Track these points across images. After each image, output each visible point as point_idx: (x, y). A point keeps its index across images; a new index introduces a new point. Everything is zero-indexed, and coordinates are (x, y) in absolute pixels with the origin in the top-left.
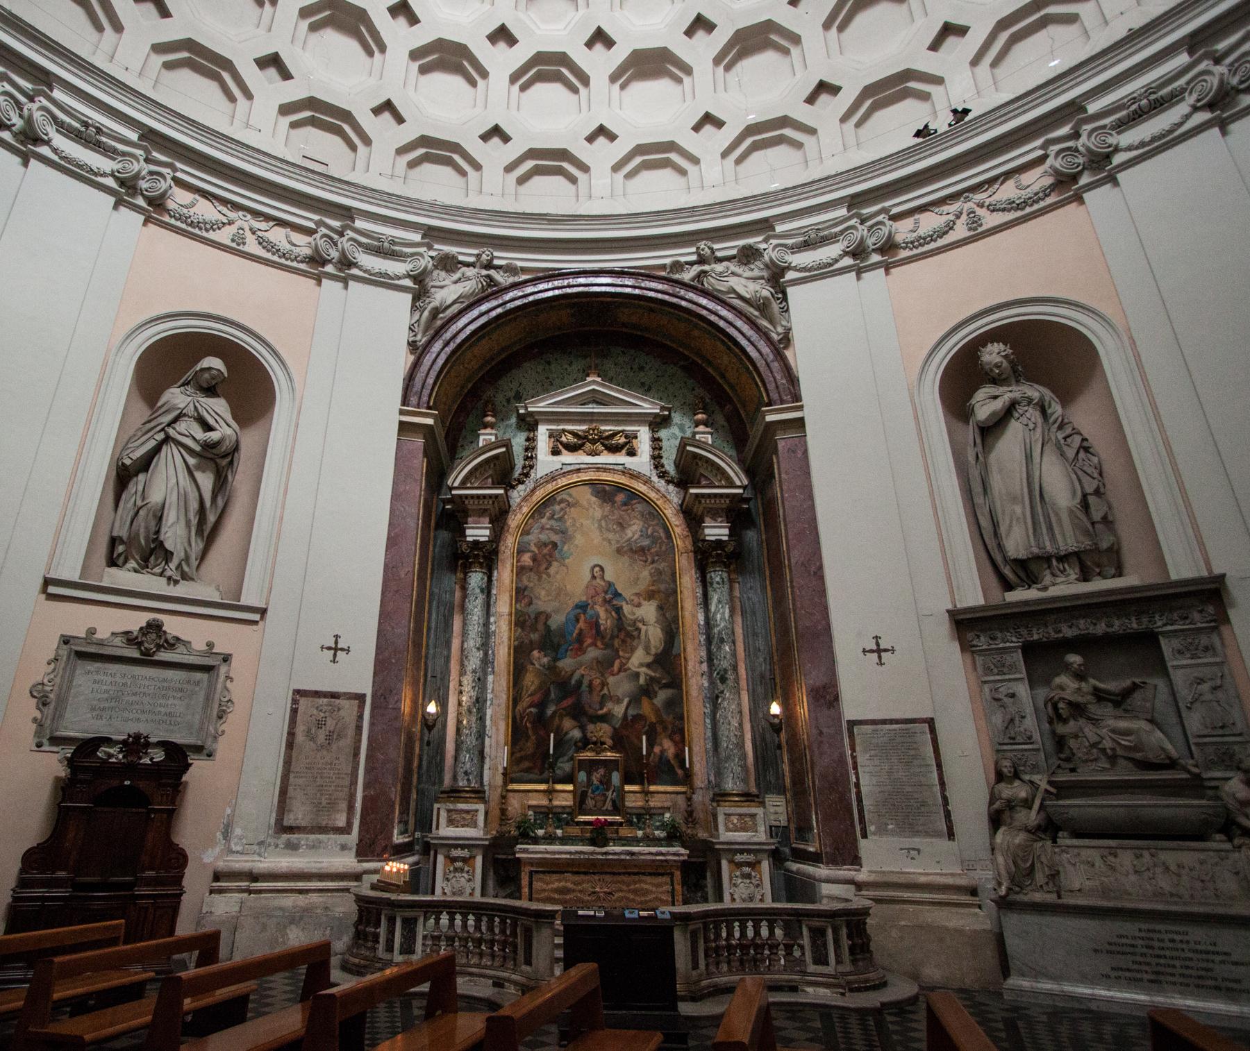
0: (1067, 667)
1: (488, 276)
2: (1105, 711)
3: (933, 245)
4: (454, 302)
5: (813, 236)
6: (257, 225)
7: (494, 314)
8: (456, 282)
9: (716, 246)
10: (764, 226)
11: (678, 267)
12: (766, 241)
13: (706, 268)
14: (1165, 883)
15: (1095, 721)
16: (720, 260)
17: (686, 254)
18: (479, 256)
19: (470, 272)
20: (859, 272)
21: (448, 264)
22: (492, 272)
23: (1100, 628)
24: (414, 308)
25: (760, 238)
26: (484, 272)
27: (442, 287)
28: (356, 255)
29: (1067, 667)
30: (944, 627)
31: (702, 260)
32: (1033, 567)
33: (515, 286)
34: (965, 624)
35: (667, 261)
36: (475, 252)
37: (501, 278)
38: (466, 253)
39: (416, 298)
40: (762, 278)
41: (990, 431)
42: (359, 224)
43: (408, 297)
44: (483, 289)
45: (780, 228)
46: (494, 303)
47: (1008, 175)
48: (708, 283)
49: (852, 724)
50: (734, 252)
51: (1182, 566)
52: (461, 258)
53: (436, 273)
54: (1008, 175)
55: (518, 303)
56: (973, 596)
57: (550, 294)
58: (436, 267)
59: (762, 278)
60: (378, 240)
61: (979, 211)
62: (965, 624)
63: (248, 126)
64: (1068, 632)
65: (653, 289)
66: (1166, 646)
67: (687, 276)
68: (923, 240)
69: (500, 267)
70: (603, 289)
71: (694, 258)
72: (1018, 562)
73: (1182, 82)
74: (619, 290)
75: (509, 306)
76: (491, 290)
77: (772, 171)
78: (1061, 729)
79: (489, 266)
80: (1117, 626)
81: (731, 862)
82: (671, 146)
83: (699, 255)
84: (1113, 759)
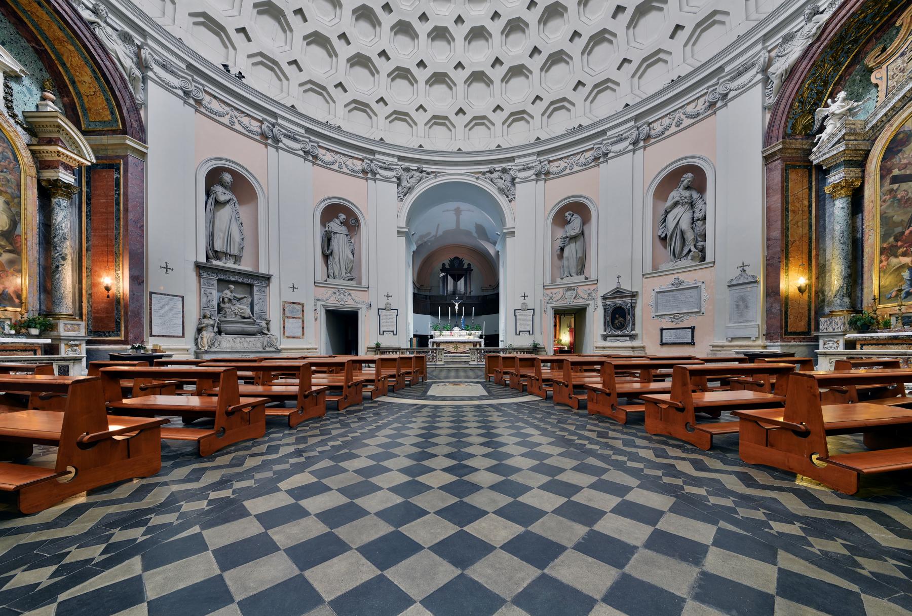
0: (229, 288)
2: (235, 302)
3: (214, 116)
14: (246, 345)
15: (233, 304)
23: (240, 280)
29: (229, 288)
30: (192, 266)
32: (220, 255)
34: (199, 267)
41: (218, 204)
47: (248, 115)
49: (151, 293)
51: (263, 270)
54: (248, 115)
56: (202, 259)
61: (236, 121)
62: (199, 267)
64: (232, 279)
66: (255, 289)
68: (212, 112)
72: (216, 252)
73: (302, 139)
78: (222, 305)
80: (245, 281)
81: (67, 344)
84: (236, 315)
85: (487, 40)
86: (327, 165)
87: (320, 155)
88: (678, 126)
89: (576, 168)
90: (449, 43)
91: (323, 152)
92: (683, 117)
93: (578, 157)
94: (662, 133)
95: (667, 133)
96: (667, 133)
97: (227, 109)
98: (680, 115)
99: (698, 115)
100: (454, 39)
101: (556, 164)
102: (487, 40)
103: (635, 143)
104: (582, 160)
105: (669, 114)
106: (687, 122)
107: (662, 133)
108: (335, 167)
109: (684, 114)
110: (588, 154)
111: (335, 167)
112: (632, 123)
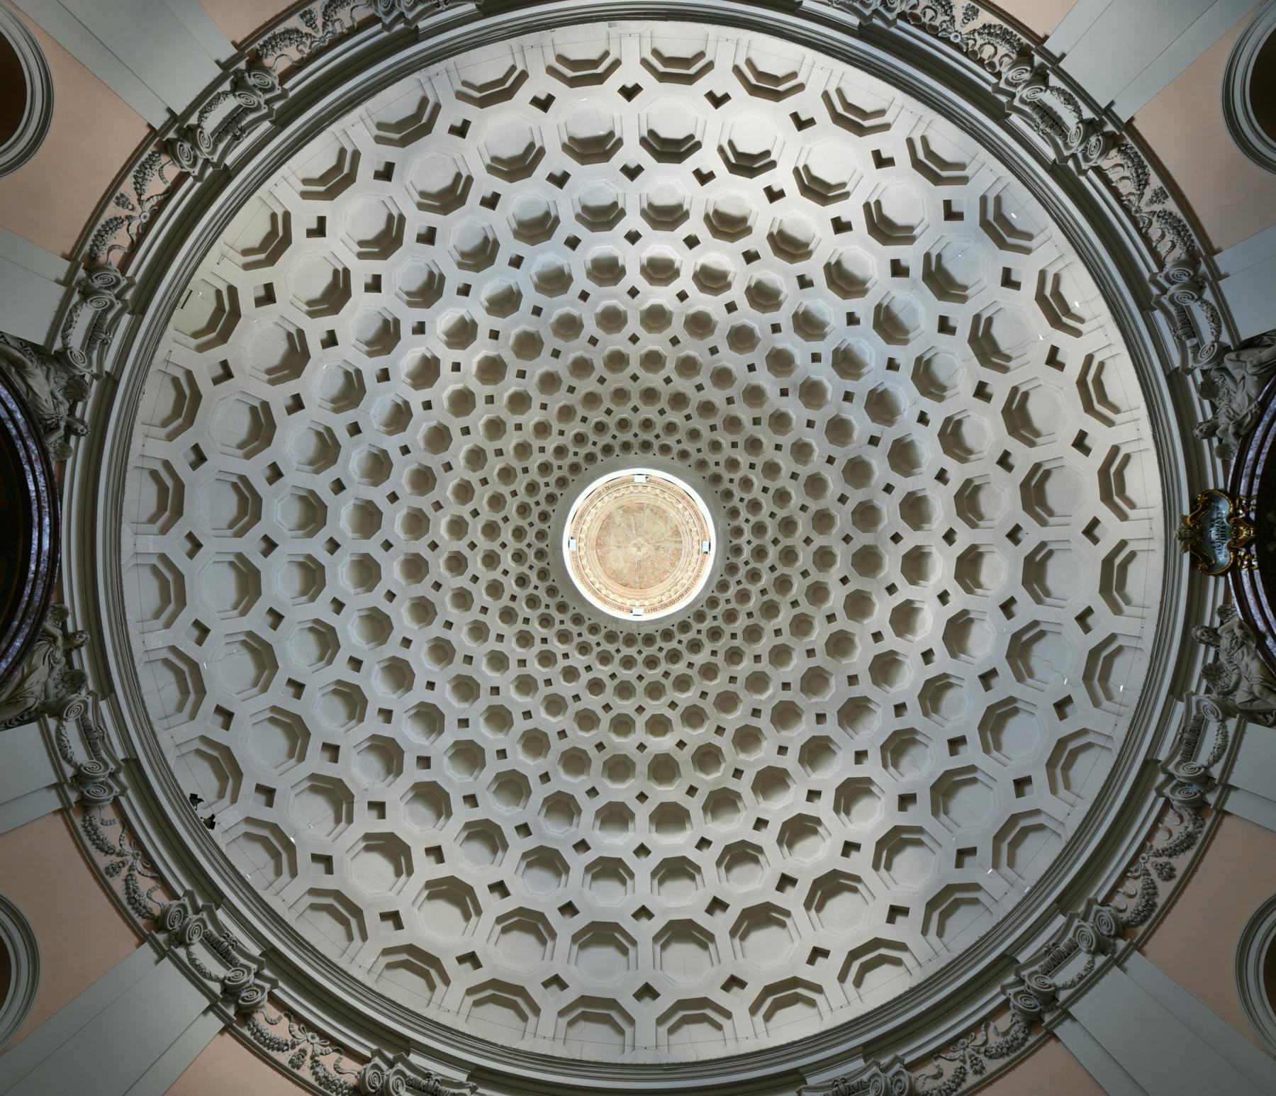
1: (57, 427)
4: (29, 387)
5: (96, 734)
6: (135, 225)
7: (10, 425)
8: (52, 394)
9: (83, 649)
10: (106, 689)
11: (62, 614)
12: (89, 693)
13: (60, 641)
16: (68, 654)
17: (76, 621)
18: (82, 422)
19: (64, 409)
20: (58, 787)
21: (75, 390)
22: (61, 432)
24: (25, 345)
25: (91, 687)
26: (63, 424)
27: (47, 378)
28: (94, 304)
31: (66, 635)
33: (44, 453)
35: (67, 604)
36: (86, 419)
37: (54, 440)
38: (85, 410)
39: (35, 347)
40: (47, 697)
42: (126, 318)
43: (40, 340)
44: (42, 419)
45: (103, 705)
46: (23, 428)
48: (41, 648)
50: (77, 666)
52: (80, 405)
53: (66, 376)
55: (22, 453)
57: (32, 487)
58: (72, 377)
59: (47, 697)
60: (109, 330)
63: (223, 256)
65: (32, 593)
67: (50, 625)
69: (67, 440)
70: (35, 542)
71: (70, 629)
74: (34, 558)
75: (19, 443)
76: (39, 427)
77: (159, 689)
79: (70, 430)
82: (182, 602)
83: (74, 634)
85: (693, 878)
86: (261, 1048)
87: (259, 1018)
88: (1170, 877)
89: (992, 1066)
90: (624, 882)
91: (272, 1012)
92: (1163, 860)
93: (980, 1038)
94: (1150, 906)
95: (1160, 901)
96: (1160, 901)
97: (127, 848)
98: (1149, 863)
99: (1189, 841)
100: (632, 876)
101: (930, 1069)
102: (693, 878)
103: (1101, 947)
104: (995, 1041)
105: (1126, 870)
106: (1181, 863)
107: (1150, 906)
108: (284, 1058)
109: (1158, 854)
110: (1004, 1022)
111: (284, 1058)
112: (1060, 920)
